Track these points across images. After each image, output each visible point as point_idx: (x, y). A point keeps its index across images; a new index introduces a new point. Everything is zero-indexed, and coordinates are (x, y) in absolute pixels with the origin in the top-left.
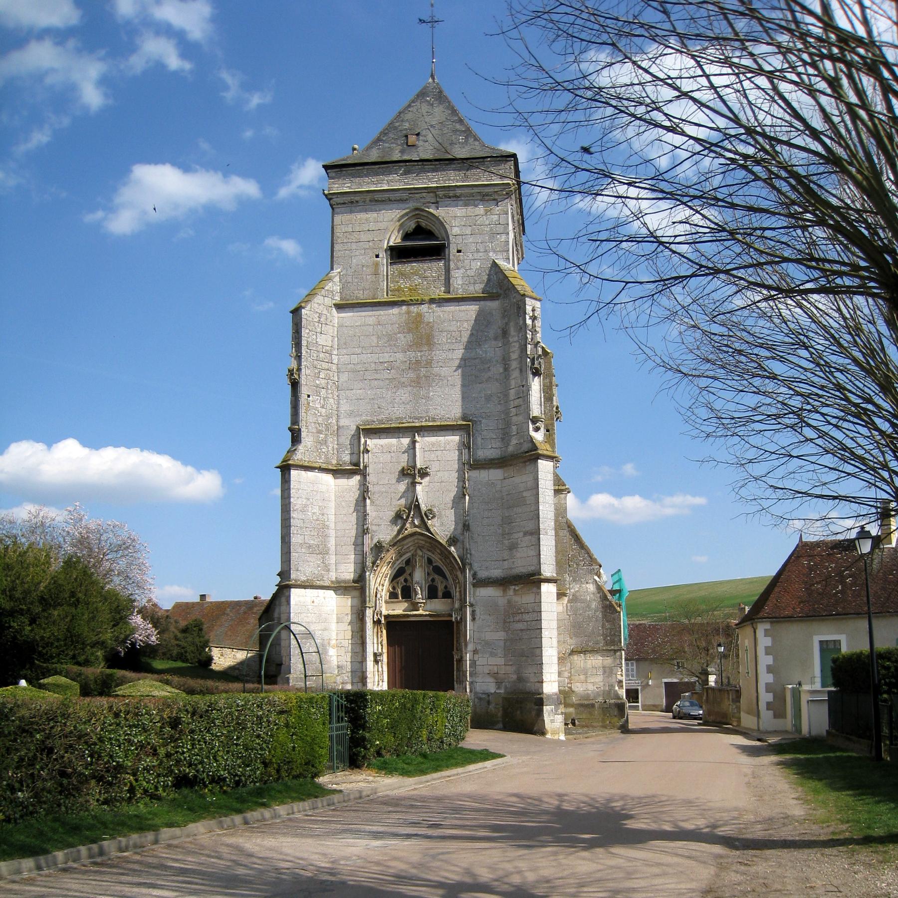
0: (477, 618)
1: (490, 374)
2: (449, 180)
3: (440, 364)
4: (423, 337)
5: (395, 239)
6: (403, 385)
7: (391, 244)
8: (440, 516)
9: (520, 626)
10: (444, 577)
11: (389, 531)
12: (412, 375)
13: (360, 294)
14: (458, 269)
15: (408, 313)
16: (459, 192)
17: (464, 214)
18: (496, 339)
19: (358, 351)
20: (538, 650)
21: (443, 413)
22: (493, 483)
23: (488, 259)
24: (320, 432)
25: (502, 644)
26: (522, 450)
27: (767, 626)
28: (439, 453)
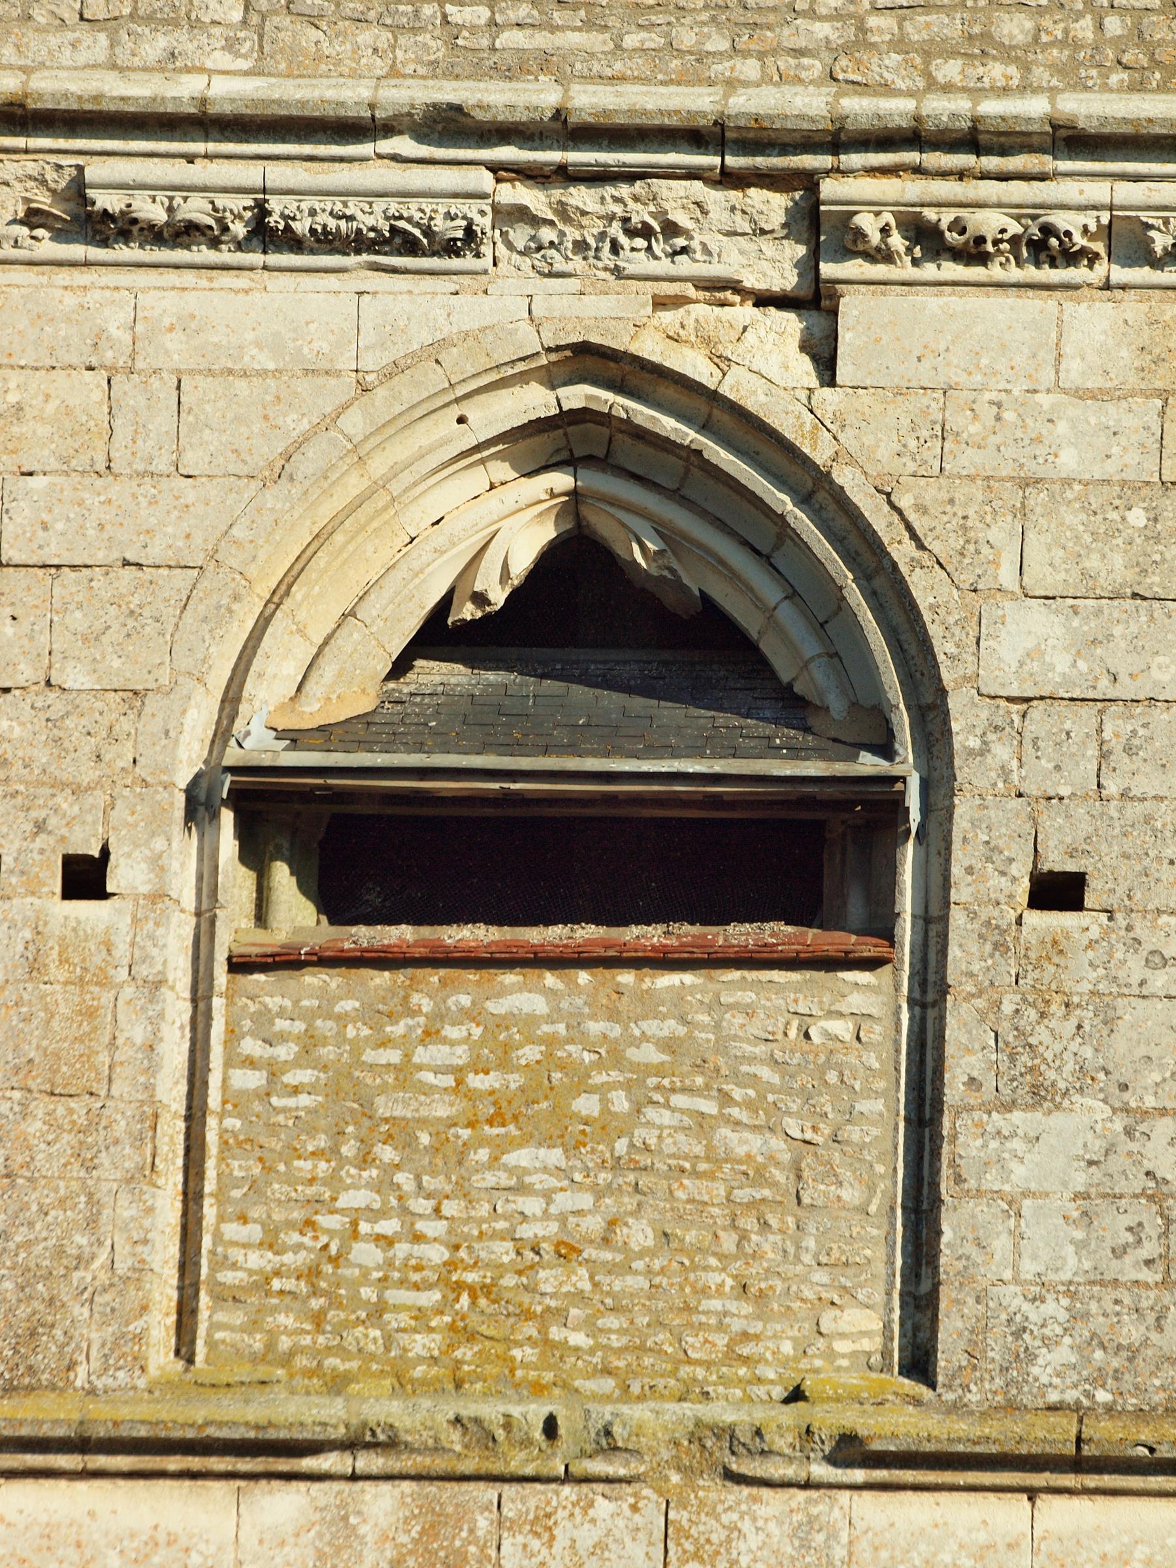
2: (982, 46)
7: (257, 744)
14: (1041, 1095)
17: (1131, 460)
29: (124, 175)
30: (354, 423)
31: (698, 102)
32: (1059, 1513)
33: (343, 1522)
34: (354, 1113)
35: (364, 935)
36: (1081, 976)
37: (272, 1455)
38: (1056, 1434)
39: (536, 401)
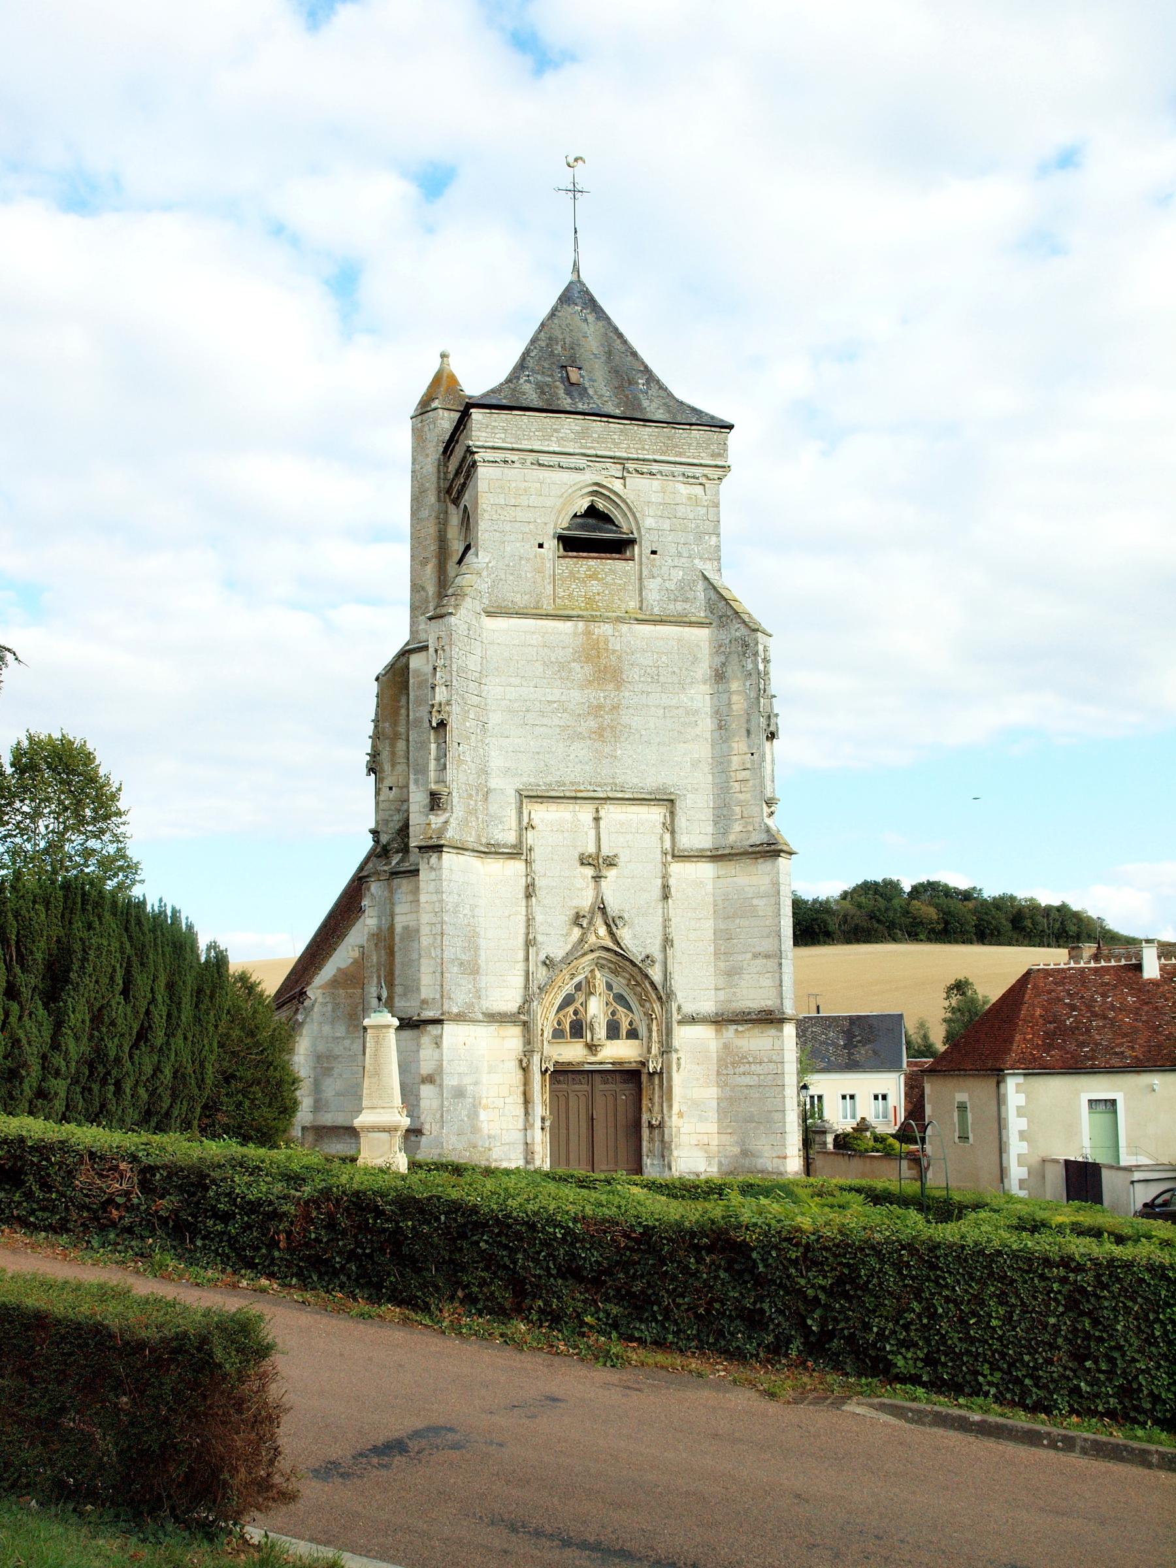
0: (682, 1066)
1: (698, 730)
2: (643, 449)
3: (631, 711)
4: (605, 669)
6: (579, 736)
9: (747, 1080)
10: (630, 1009)
11: (562, 944)
12: (592, 723)
13: (518, 598)
15: (588, 633)
16: (655, 467)
18: (705, 683)
19: (517, 681)
20: (777, 1116)
21: (635, 781)
22: (701, 882)
23: (693, 568)
25: (714, 1104)
26: (751, 842)
27: (1021, 1079)
29: (544, 459)
31: (611, 454)
32: (658, 627)
35: (570, 554)
36: (658, 563)
37: (568, 618)
38: (658, 618)
39: (591, 489)
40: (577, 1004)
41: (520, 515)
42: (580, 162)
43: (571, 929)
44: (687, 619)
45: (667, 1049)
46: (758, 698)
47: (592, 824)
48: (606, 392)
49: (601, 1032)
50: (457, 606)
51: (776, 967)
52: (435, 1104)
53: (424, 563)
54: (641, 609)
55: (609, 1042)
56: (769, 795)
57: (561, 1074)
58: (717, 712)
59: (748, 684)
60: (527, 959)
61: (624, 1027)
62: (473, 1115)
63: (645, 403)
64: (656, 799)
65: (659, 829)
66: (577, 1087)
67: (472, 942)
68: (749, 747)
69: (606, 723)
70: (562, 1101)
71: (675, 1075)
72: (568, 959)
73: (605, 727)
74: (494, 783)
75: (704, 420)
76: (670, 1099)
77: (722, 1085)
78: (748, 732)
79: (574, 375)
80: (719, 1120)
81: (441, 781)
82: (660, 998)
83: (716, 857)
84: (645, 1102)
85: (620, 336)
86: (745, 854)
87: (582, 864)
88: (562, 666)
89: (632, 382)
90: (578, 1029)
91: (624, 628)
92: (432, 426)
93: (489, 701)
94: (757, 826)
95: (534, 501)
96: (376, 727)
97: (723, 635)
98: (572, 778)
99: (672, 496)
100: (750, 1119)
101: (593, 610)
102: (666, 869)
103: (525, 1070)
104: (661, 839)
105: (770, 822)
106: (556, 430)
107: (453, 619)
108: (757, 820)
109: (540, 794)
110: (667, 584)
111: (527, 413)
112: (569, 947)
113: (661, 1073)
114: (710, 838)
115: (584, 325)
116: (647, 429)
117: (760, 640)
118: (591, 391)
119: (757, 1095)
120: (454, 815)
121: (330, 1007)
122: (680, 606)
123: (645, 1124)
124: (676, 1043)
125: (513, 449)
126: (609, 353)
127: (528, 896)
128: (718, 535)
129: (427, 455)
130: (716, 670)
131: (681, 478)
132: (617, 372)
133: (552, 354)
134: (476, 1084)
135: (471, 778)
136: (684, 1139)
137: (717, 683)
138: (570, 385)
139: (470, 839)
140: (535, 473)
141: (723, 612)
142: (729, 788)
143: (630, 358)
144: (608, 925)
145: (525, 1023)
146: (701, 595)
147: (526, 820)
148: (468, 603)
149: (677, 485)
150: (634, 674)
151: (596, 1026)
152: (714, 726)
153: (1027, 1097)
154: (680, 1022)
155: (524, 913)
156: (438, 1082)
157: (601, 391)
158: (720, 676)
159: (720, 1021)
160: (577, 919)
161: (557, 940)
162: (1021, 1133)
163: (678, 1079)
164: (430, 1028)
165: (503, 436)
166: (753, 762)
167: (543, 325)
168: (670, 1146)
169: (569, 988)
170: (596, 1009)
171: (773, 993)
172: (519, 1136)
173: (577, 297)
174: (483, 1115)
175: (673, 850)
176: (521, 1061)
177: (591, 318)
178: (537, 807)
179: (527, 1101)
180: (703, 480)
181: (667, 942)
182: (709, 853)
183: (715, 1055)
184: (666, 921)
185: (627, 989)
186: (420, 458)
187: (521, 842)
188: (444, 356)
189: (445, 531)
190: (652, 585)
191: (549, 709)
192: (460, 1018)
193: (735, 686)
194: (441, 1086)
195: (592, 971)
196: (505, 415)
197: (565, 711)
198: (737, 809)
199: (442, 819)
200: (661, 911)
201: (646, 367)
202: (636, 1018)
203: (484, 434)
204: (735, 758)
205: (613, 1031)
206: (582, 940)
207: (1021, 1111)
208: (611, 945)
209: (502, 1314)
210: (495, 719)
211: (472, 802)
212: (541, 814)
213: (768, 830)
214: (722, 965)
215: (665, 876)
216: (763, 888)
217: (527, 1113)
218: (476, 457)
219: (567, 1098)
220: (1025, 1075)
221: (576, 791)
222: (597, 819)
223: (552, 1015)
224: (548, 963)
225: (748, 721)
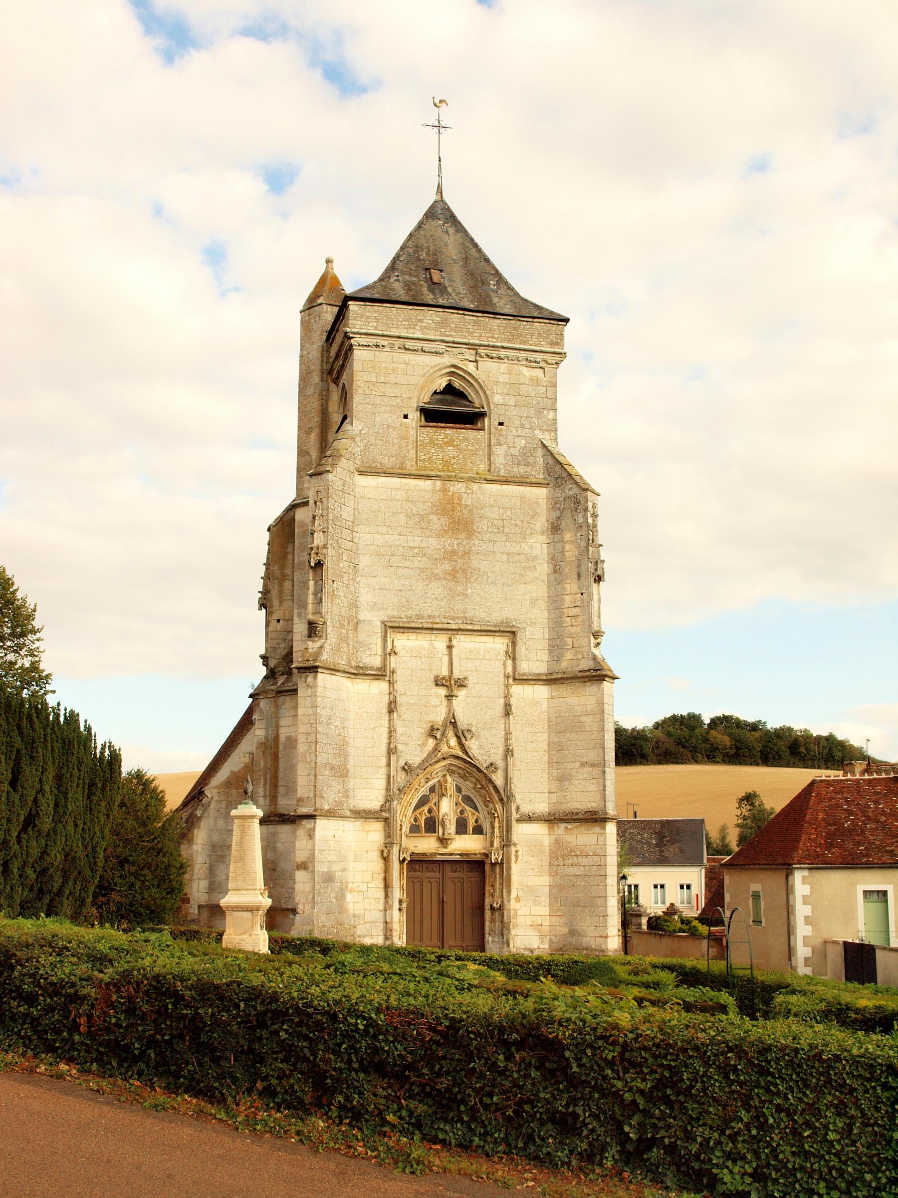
0: (520, 859)
2: (494, 338)
4: (458, 521)
5: (425, 398)
6: (436, 577)
8: (478, 738)
9: (574, 870)
11: (418, 752)
12: (447, 566)
13: (385, 461)
14: (500, 445)
15: (444, 490)
16: (503, 353)
17: (507, 381)
18: (543, 534)
19: (383, 530)
20: (599, 901)
21: (483, 615)
22: (538, 702)
23: (534, 438)
24: (342, 626)
25: (546, 890)
26: (580, 668)
27: (806, 873)
28: (477, 663)
29: (409, 344)
30: (431, 371)
32: (504, 487)
33: (435, 485)
34: (432, 442)
35: (431, 424)
36: (504, 433)
37: (428, 477)
38: (504, 479)
39: (448, 370)
40: (431, 804)
41: (389, 391)
42: (444, 104)
43: (427, 740)
44: (528, 480)
45: (507, 843)
46: (587, 547)
47: (446, 651)
48: (463, 291)
49: (451, 828)
50: (333, 465)
51: (600, 774)
52: (308, 887)
53: (309, 432)
54: (489, 471)
55: (457, 837)
56: (596, 629)
57: (417, 864)
58: (553, 558)
59: (579, 535)
60: (389, 765)
61: (471, 824)
62: (341, 897)
63: (495, 300)
64: (500, 631)
65: (502, 657)
66: (430, 874)
67: (342, 750)
68: (579, 587)
69: (458, 566)
70: (417, 886)
71: (513, 865)
72: (425, 765)
73: (457, 570)
74: (363, 615)
75: (545, 315)
76: (509, 886)
77: (553, 874)
78: (579, 575)
79: (436, 276)
80: (551, 904)
81: (318, 612)
82: (501, 800)
83: (551, 680)
84: (488, 888)
85: (476, 245)
86: (574, 678)
87: (437, 685)
88: (422, 518)
89: (484, 283)
90: (431, 825)
91: (475, 487)
92: (317, 319)
93: (360, 546)
94: (585, 655)
95: (400, 379)
96: (267, 569)
97: (559, 494)
98: (429, 612)
99: (517, 377)
100: (576, 904)
101: (449, 471)
102: (508, 690)
103: (386, 859)
104: (504, 664)
105: (596, 651)
106: (420, 321)
107: (330, 476)
108: (586, 649)
109: (401, 625)
110: (512, 451)
111: (396, 306)
112: (425, 755)
113: (502, 863)
114: (545, 665)
115: (445, 236)
116: (497, 321)
117: (590, 499)
118: (450, 290)
119: (583, 883)
120: (329, 642)
121: (223, 805)
122: (522, 470)
123: (487, 907)
124: (515, 838)
125: (383, 336)
126: (466, 259)
127: (391, 712)
128: (555, 410)
129: (313, 343)
130: (553, 523)
131: (524, 363)
132: (472, 274)
133: (418, 259)
134: (344, 870)
135: (343, 611)
136: (520, 920)
137: (553, 534)
138: (433, 285)
139: (342, 663)
140: (401, 356)
141: (559, 475)
142: (562, 622)
143: (483, 263)
144: (458, 737)
145: (386, 820)
146: (540, 461)
147: (389, 647)
148: (343, 463)
149: (521, 368)
150: (483, 525)
151: (447, 823)
152: (550, 571)
153: (811, 888)
154: (518, 821)
155: (387, 726)
156: (310, 869)
157: (458, 287)
158: (555, 528)
159: (552, 820)
160: (432, 732)
161: (414, 750)
162: (806, 918)
163: (517, 871)
164: (305, 822)
165: (375, 324)
166: (582, 600)
167: (411, 235)
168: (509, 925)
169: (424, 790)
170: (447, 808)
171: (598, 796)
172: (379, 916)
173: (440, 213)
174: (349, 897)
175: (514, 674)
176: (382, 851)
177: (451, 231)
178: (399, 636)
179: (387, 886)
180: (543, 365)
181: (508, 752)
182: (545, 677)
183: (548, 848)
184: (508, 735)
185: (473, 791)
186: (308, 345)
187: (385, 665)
188: (328, 261)
189: (327, 406)
190: (499, 452)
191: (411, 554)
192: (330, 814)
193: (568, 536)
194: (313, 872)
195: (444, 776)
196: (377, 307)
197: (424, 555)
198: (569, 640)
199: (318, 644)
200: (503, 726)
201: (497, 271)
202: (481, 816)
203: (359, 323)
204: (567, 598)
205: (462, 828)
206: (436, 749)
207: (806, 900)
208: (460, 753)
209: (298, 1107)
210: (364, 561)
211: (344, 631)
212: (402, 642)
213: (595, 658)
214: (554, 772)
215: (507, 696)
216: (589, 707)
217: (387, 896)
218: (352, 341)
219: (422, 885)
220: (810, 869)
221: (432, 623)
222: (450, 647)
223: (409, 813)
224: (407, 769)
225: (579, 566)
